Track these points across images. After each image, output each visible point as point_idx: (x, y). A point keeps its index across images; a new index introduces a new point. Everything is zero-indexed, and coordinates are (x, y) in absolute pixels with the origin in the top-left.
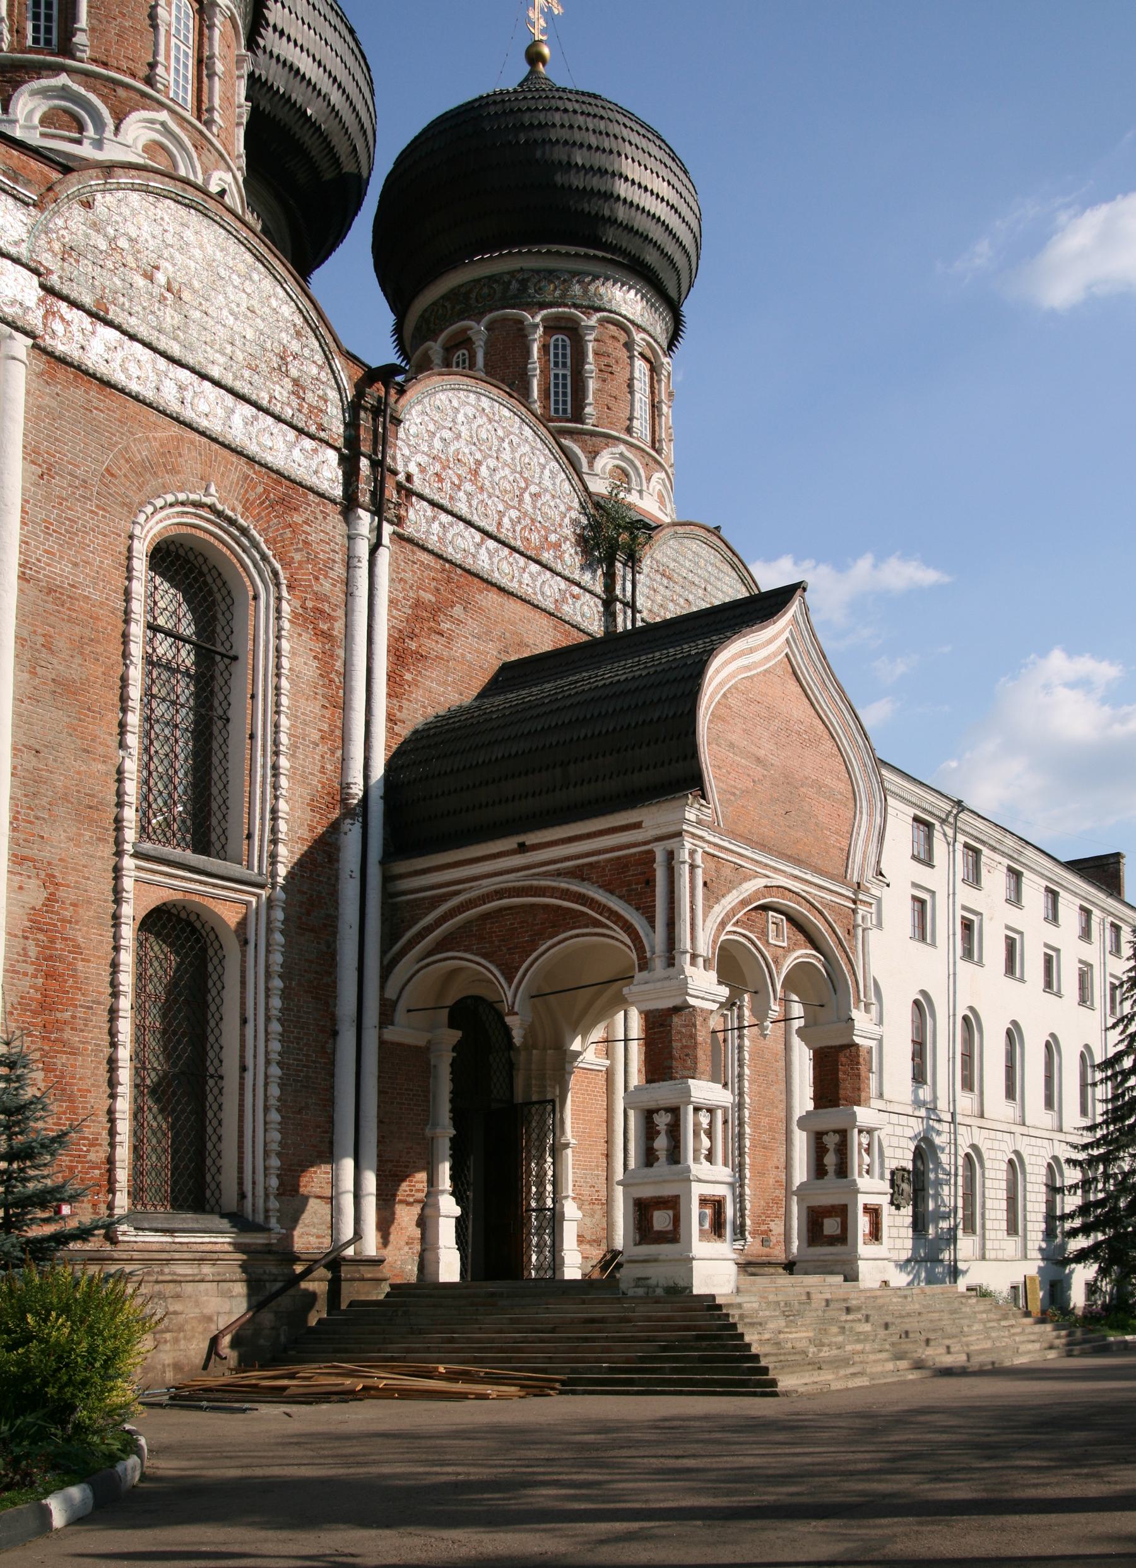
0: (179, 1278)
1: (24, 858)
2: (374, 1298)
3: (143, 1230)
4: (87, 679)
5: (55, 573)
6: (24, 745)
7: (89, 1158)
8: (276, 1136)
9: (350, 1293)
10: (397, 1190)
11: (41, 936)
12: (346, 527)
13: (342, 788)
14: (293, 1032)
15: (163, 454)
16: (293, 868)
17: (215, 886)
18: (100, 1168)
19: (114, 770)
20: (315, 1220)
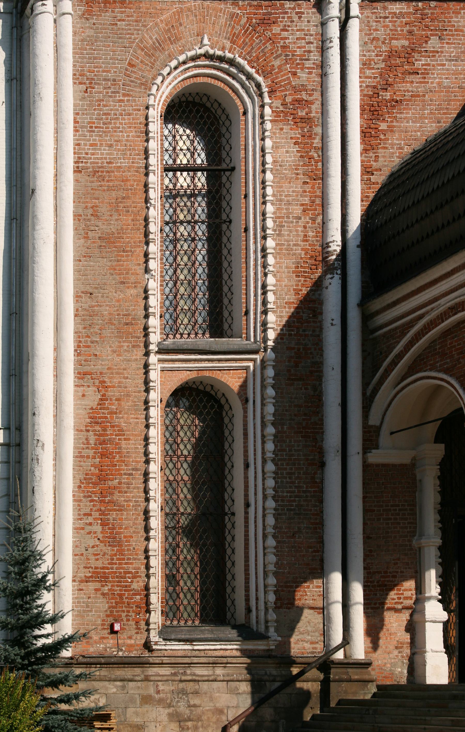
0: (197, 678)
1: (85, 374)
2: (362, 698)
3: (170, 640)
4: (122, 229)
5: (98, 158)
6: (82, 292)
7: (132, 587)
8: (272, 558)
9: (338, 693)
10: (386, 599)
11: (98, 428)
12: (318, 15)
13: (323, 249)
14: (286, 469)
15: (169, 30)
16: (282, 330)
17: (219, 360)
18: (140, 594)
19: (142, 291)
20: (309, 628)
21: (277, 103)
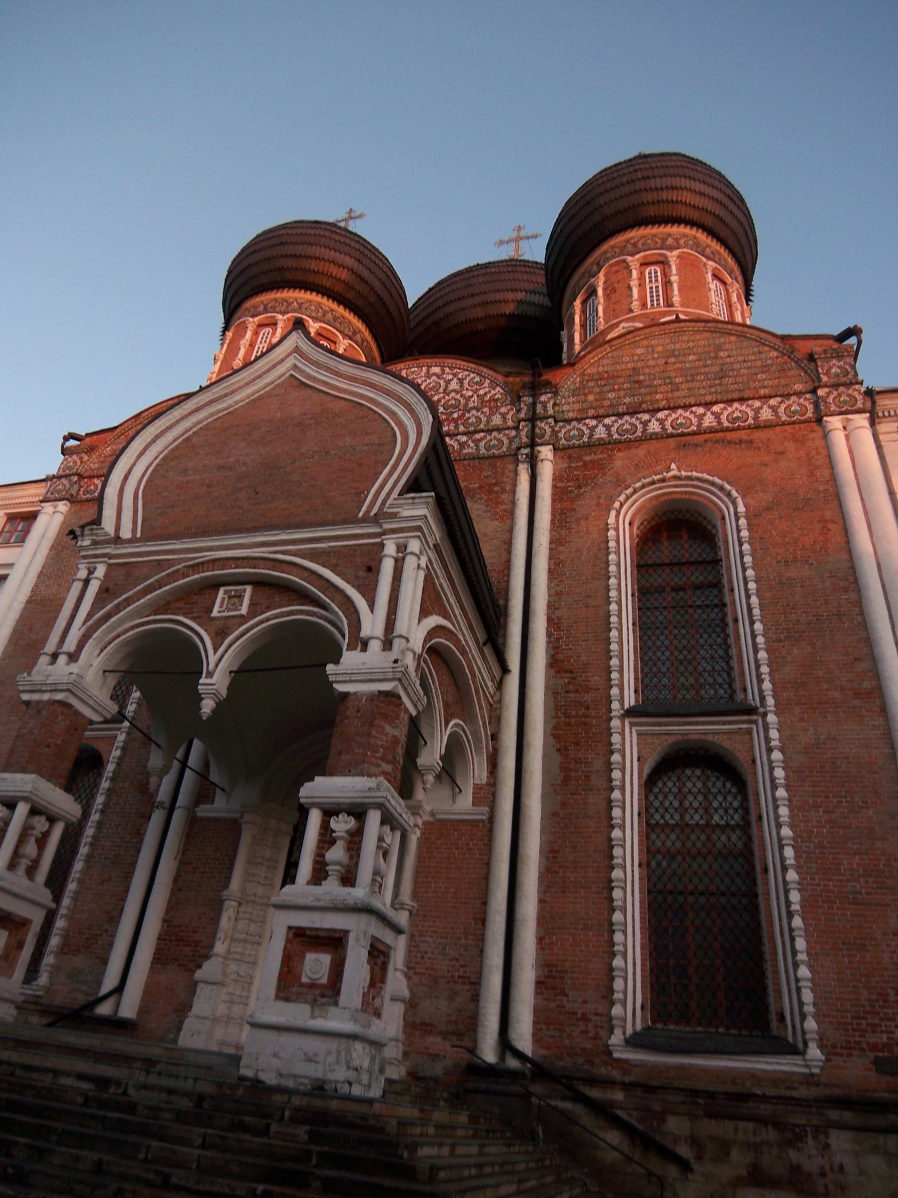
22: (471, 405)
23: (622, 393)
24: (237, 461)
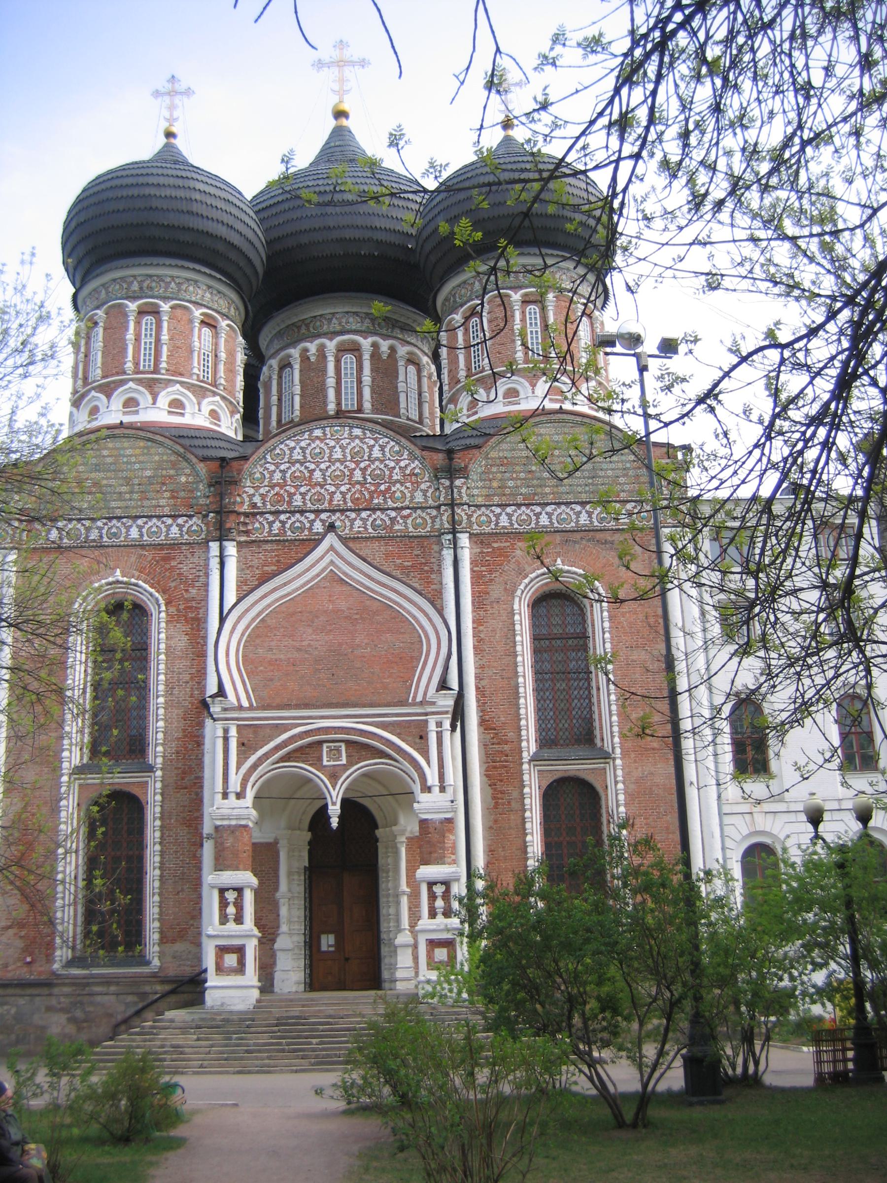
21: (172, 610)
22: (395, 477)
23: (519, 482)
24: (309, 645)
